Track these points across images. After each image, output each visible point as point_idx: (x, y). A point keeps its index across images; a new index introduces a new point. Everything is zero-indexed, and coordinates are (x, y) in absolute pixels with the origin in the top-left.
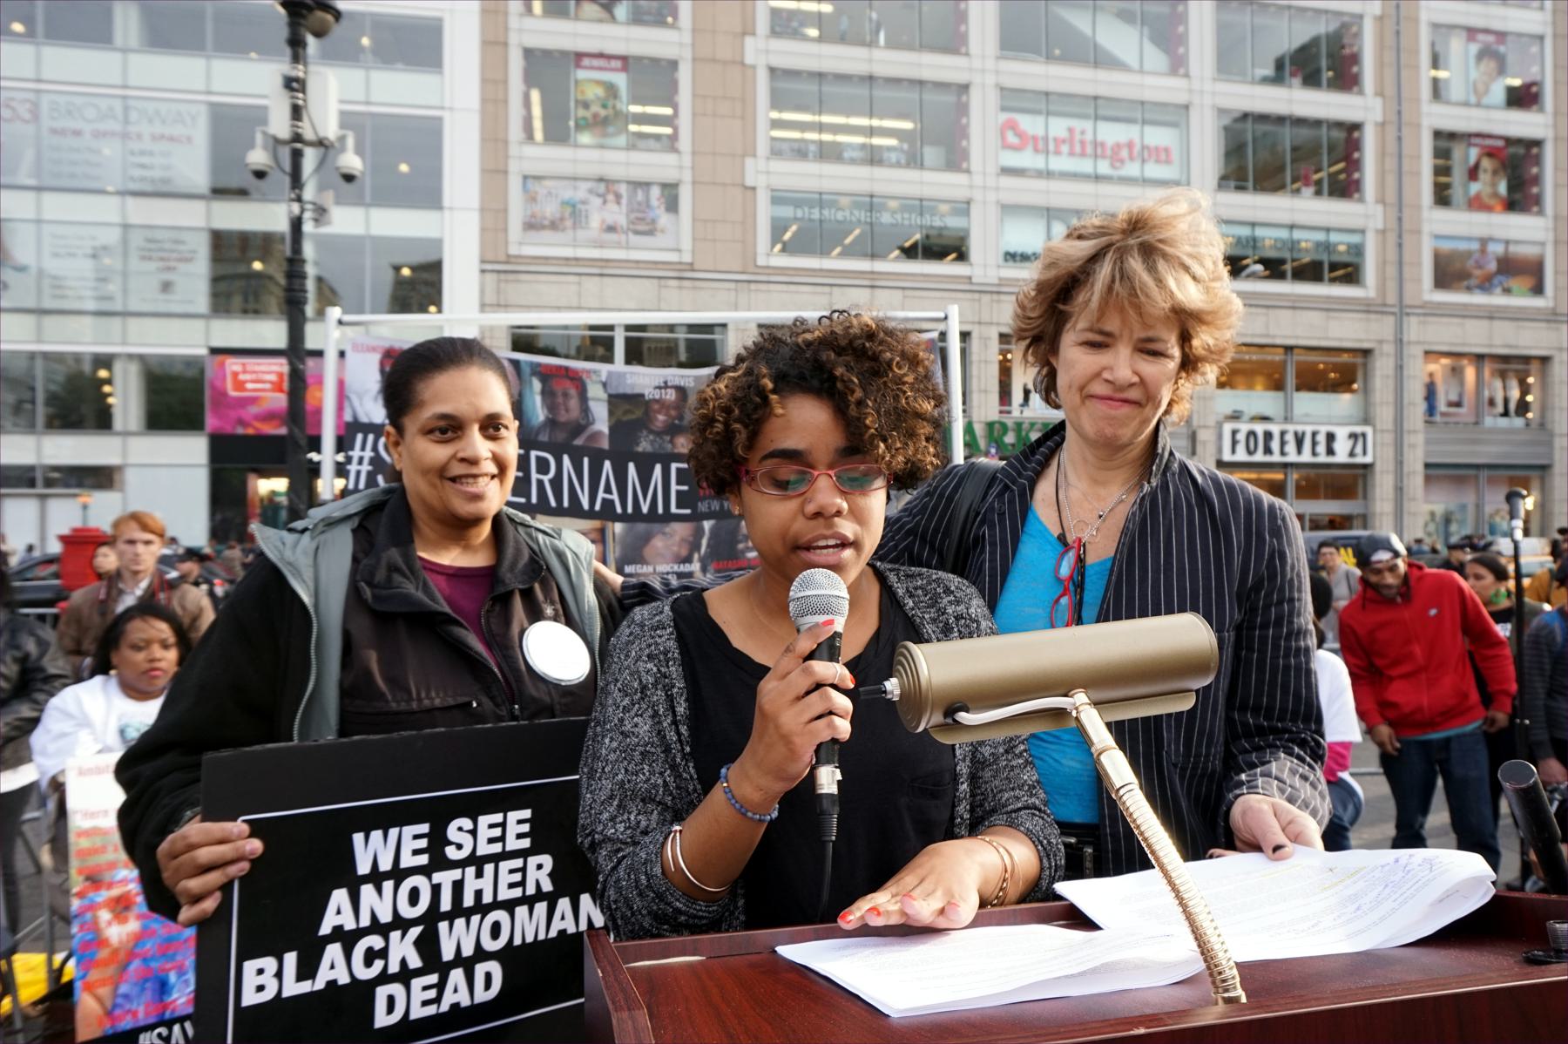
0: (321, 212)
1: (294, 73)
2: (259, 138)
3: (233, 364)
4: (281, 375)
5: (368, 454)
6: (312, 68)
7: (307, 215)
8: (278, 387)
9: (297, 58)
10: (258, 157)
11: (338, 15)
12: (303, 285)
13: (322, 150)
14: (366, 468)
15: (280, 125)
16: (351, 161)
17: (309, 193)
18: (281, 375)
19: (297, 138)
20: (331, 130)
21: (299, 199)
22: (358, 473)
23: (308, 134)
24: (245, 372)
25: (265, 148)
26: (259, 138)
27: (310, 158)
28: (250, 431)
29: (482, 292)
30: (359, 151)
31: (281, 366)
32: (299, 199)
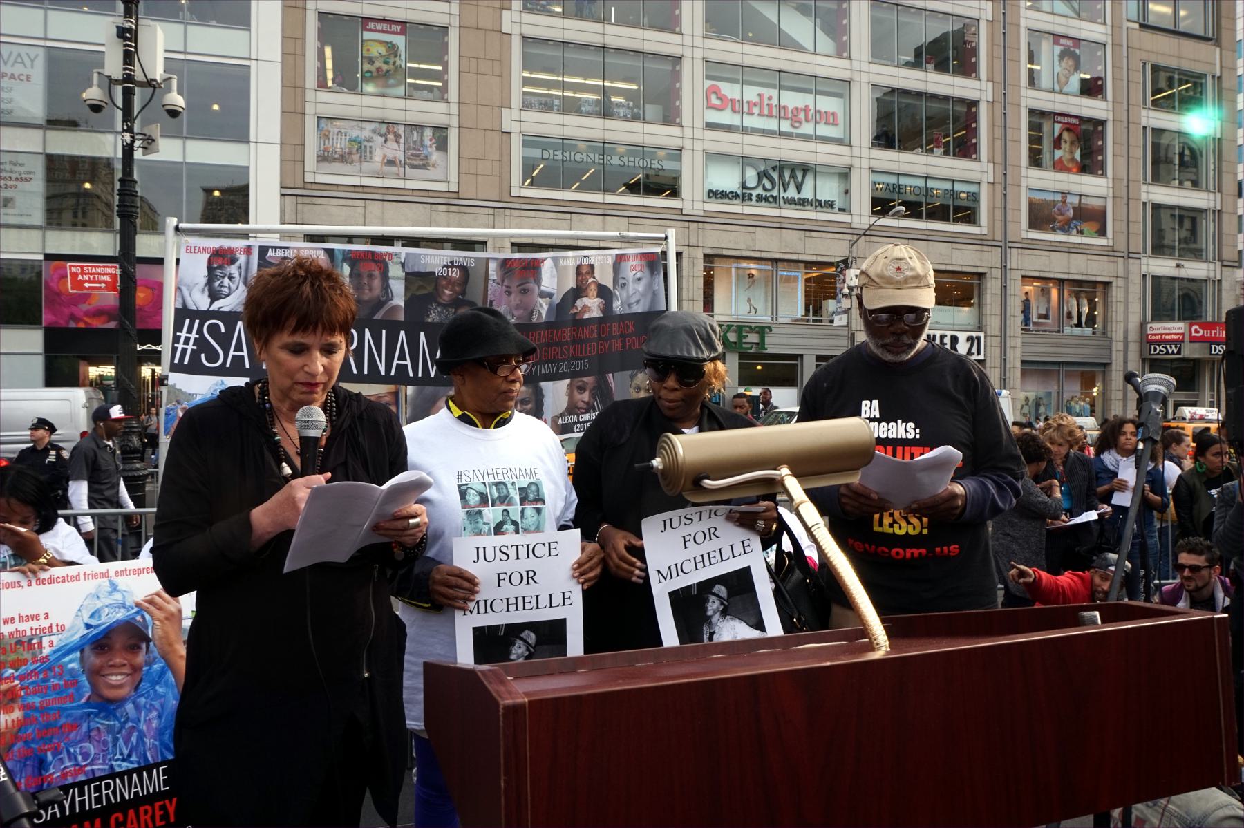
1: (127, 25)
2: (95, 76)
3: (73, 268)
4: (114, 276)
6: (141, 22)
7: (137, 144)
8: (110, 286)
9: (128, 13)
10: (93, 93)
12: (133, 201)
13: (151, 90)
15: (114, 67)
16: (177, 100)
18: (114, 276)
19: (128, 79)
20: (158, 72)
21: (130, 130)
23: (139, 76)
24: (83, 273)
25: (99, 86)
26: (95, 76)
30: (180, 93)
31: (115, 269)
32: (130, 130)
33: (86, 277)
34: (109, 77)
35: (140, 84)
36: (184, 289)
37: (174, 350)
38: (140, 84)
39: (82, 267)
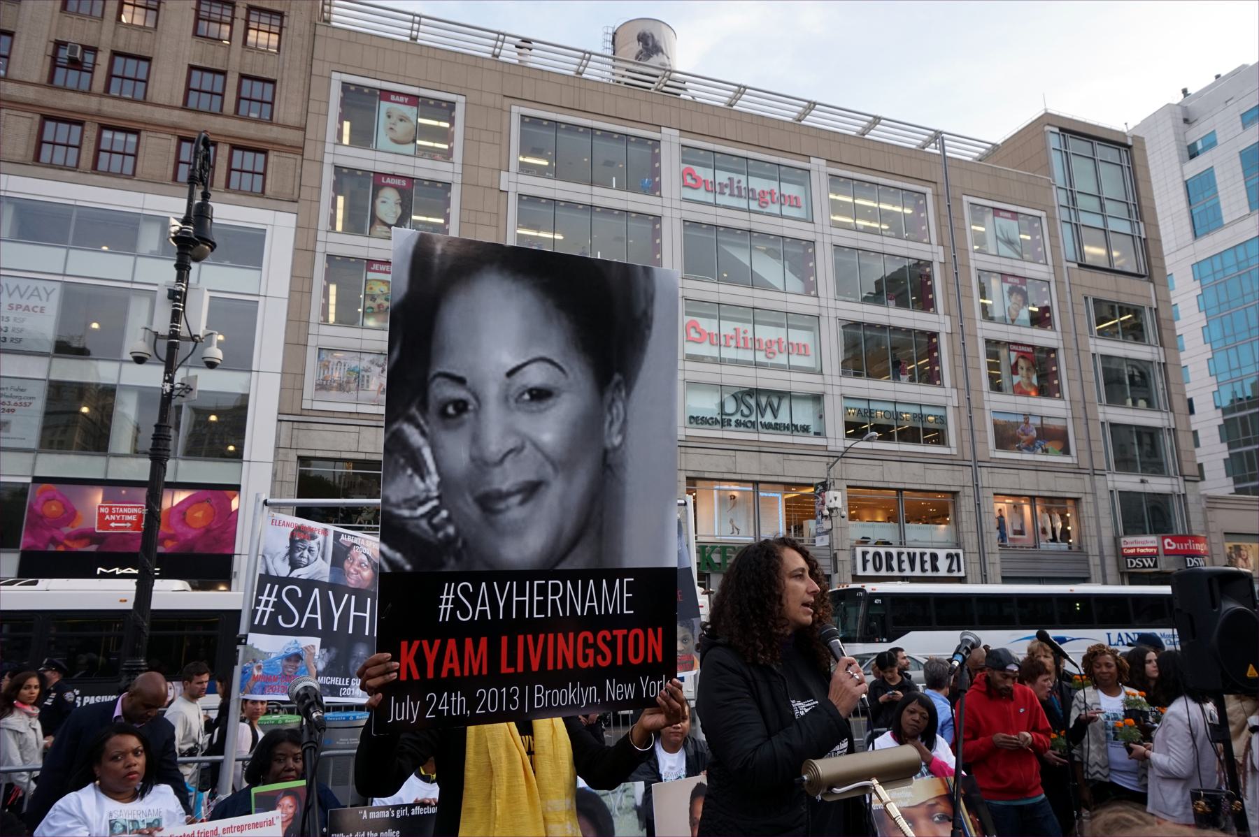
0: (187, 389)
1: (178, 289)
5: (273, 599)
7: (175, 393)
8: (136, 525)
11: (213, 246)
12: (167, 445)
13: (192, 344)
14: (269, 609)
16: (216, 353)
17: (180, 375)
19: (174, 335)
20: (201, 329)
21: (171, 380)
22: (264, 612)
23: (183, 331)
24: (110, 513)
27: (185, 347)
28: (61, 549)
29: (278, 437)
33: (113, 517)
34: (156, 333)
35: (186, 339)
36: (268, 557)
37: (254, 612)
38: (186, 339)
39: (110, 508)
